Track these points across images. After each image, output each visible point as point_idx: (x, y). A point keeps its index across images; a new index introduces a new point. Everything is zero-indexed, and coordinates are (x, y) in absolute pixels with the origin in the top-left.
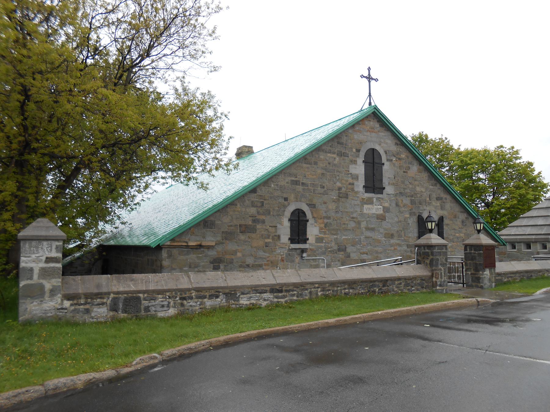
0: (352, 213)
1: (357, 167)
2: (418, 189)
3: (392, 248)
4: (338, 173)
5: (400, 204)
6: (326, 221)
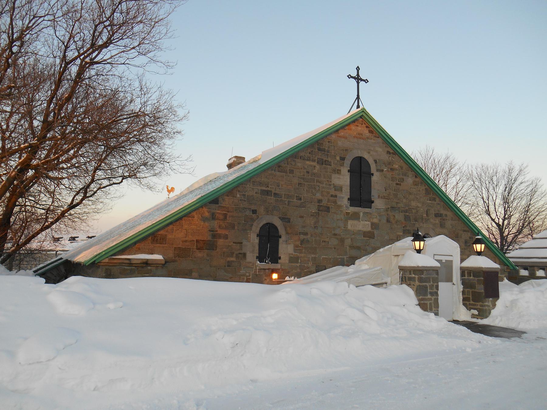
1: (341, 177)
2: (413, 204)
4: (318, 184)
5: (391, 220)
6: (302, 237)
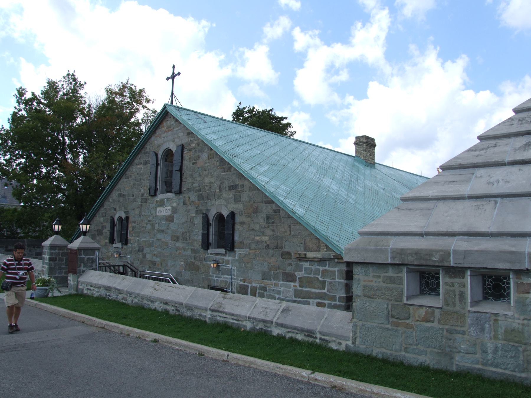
0: (149, 216)
2: (207, 180)
3: (178, 252)
